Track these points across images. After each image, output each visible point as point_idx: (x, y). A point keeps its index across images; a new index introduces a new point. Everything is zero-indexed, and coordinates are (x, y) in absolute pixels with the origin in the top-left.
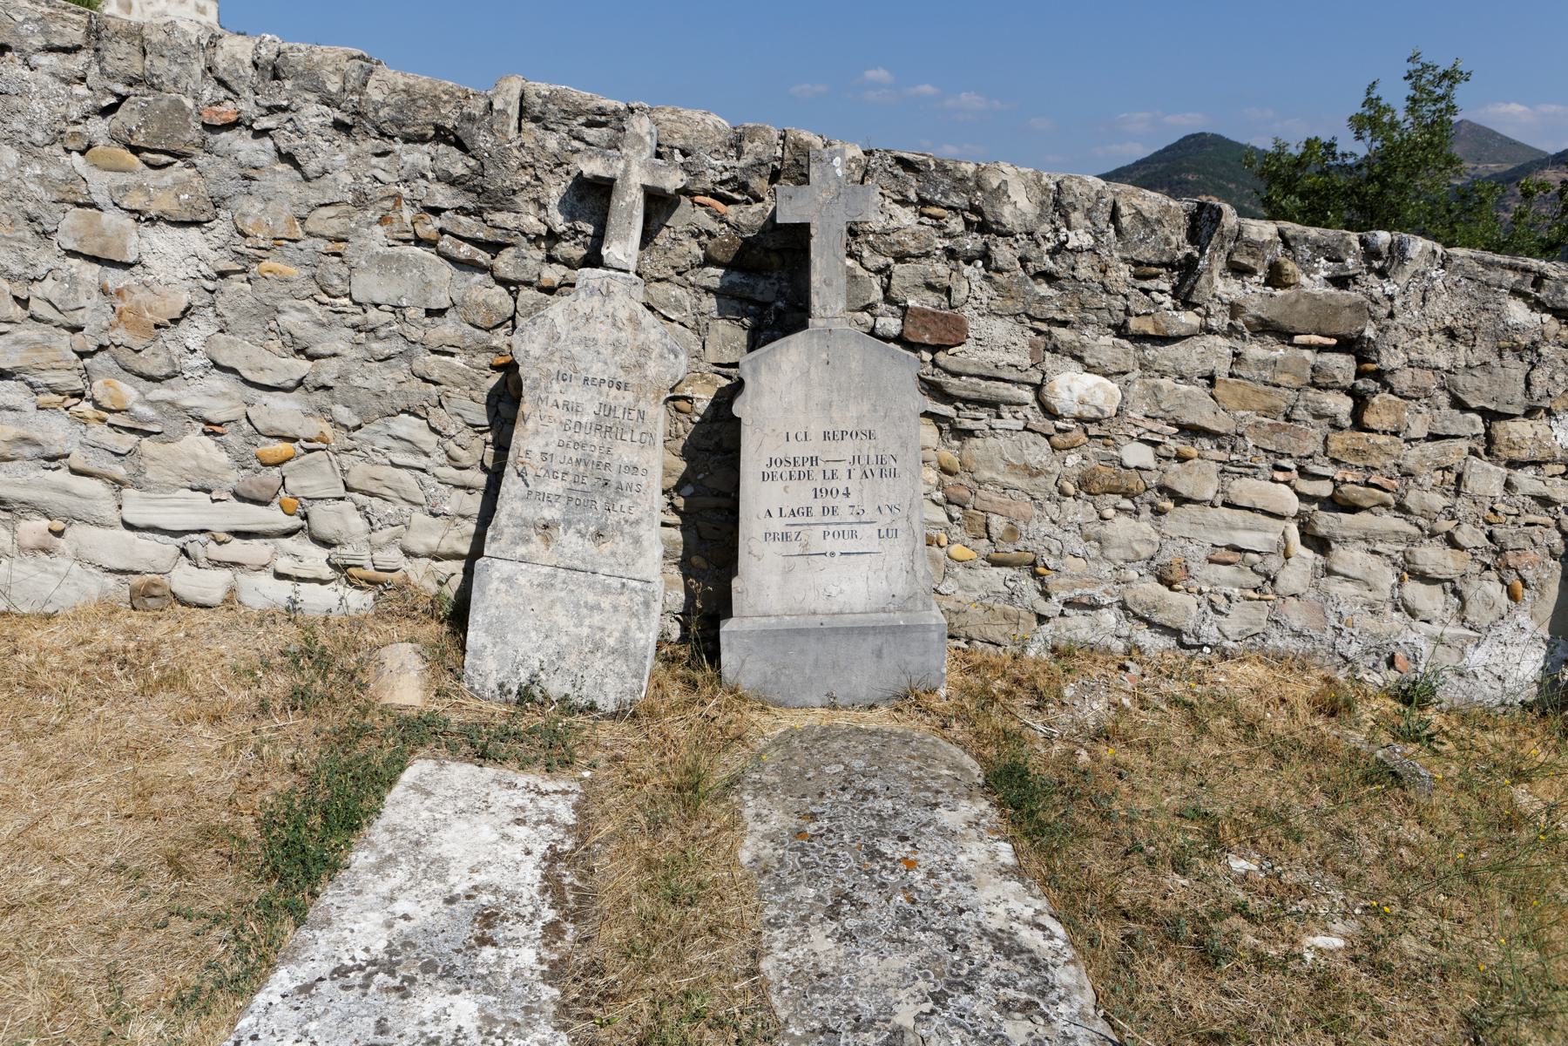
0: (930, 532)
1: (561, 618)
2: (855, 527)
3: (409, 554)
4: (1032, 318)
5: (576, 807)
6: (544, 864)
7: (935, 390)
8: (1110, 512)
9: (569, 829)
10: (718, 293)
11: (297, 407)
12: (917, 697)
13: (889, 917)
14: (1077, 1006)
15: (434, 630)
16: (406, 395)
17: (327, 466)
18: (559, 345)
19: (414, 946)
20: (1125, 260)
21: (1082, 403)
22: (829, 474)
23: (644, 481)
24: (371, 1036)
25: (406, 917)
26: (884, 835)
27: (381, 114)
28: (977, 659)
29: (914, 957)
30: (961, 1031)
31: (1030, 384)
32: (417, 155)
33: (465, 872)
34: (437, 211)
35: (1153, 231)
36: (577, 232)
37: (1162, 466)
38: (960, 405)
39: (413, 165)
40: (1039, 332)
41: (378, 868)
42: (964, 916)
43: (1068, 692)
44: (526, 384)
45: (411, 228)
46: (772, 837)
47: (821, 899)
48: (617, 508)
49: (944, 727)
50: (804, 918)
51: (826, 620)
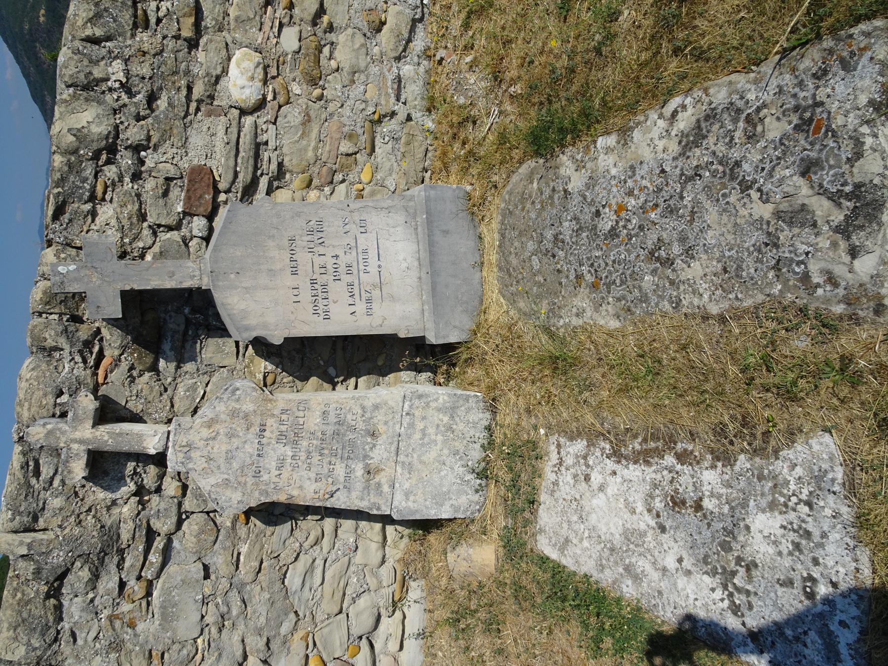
0: (353, 196)
1: (432, 454)
2: (360, 250)
3: (383, 562)
4: (187, 114)
5: (572, 439)
6: (624, 462)
7: (249, 191)
8: (333, 64)
9: (591, 444)
10: (180, 361)
11: (283, 660)
12: (474, 206)
13: (671, 223)
14: (748, 86)
15: (434, 538)
16: (271, 583)
17: (326, 630)
18: (232, 478)
19: (706, 556)
20: (133, 36)
21: (252, 78)
22: (323, 270)
23: (333, 406)
24: (795, 591)
25: (680, 560)
26: (595, 227)
27: (37, 645)
28: (438, 164)
29: (708, 204)
30: (777, 169)
31: (240, 118)
32: (73, 609)
33: (635, 517)
34: (122, 585)
35: (106, 10)
36: (135, 473)
37: (298, 21)
38: (259, 172)
39: (82, 610)
40: (198, 109)
41: (637, 578)
42: (668, 169)
43: (462, 101)
44: (264, 500)
45: (137, 603)
46: (597, 306)
47: (654, 272)
48: (354, 423)
49: (496, 187)
50: (672, 283)
51: (424, 270)
